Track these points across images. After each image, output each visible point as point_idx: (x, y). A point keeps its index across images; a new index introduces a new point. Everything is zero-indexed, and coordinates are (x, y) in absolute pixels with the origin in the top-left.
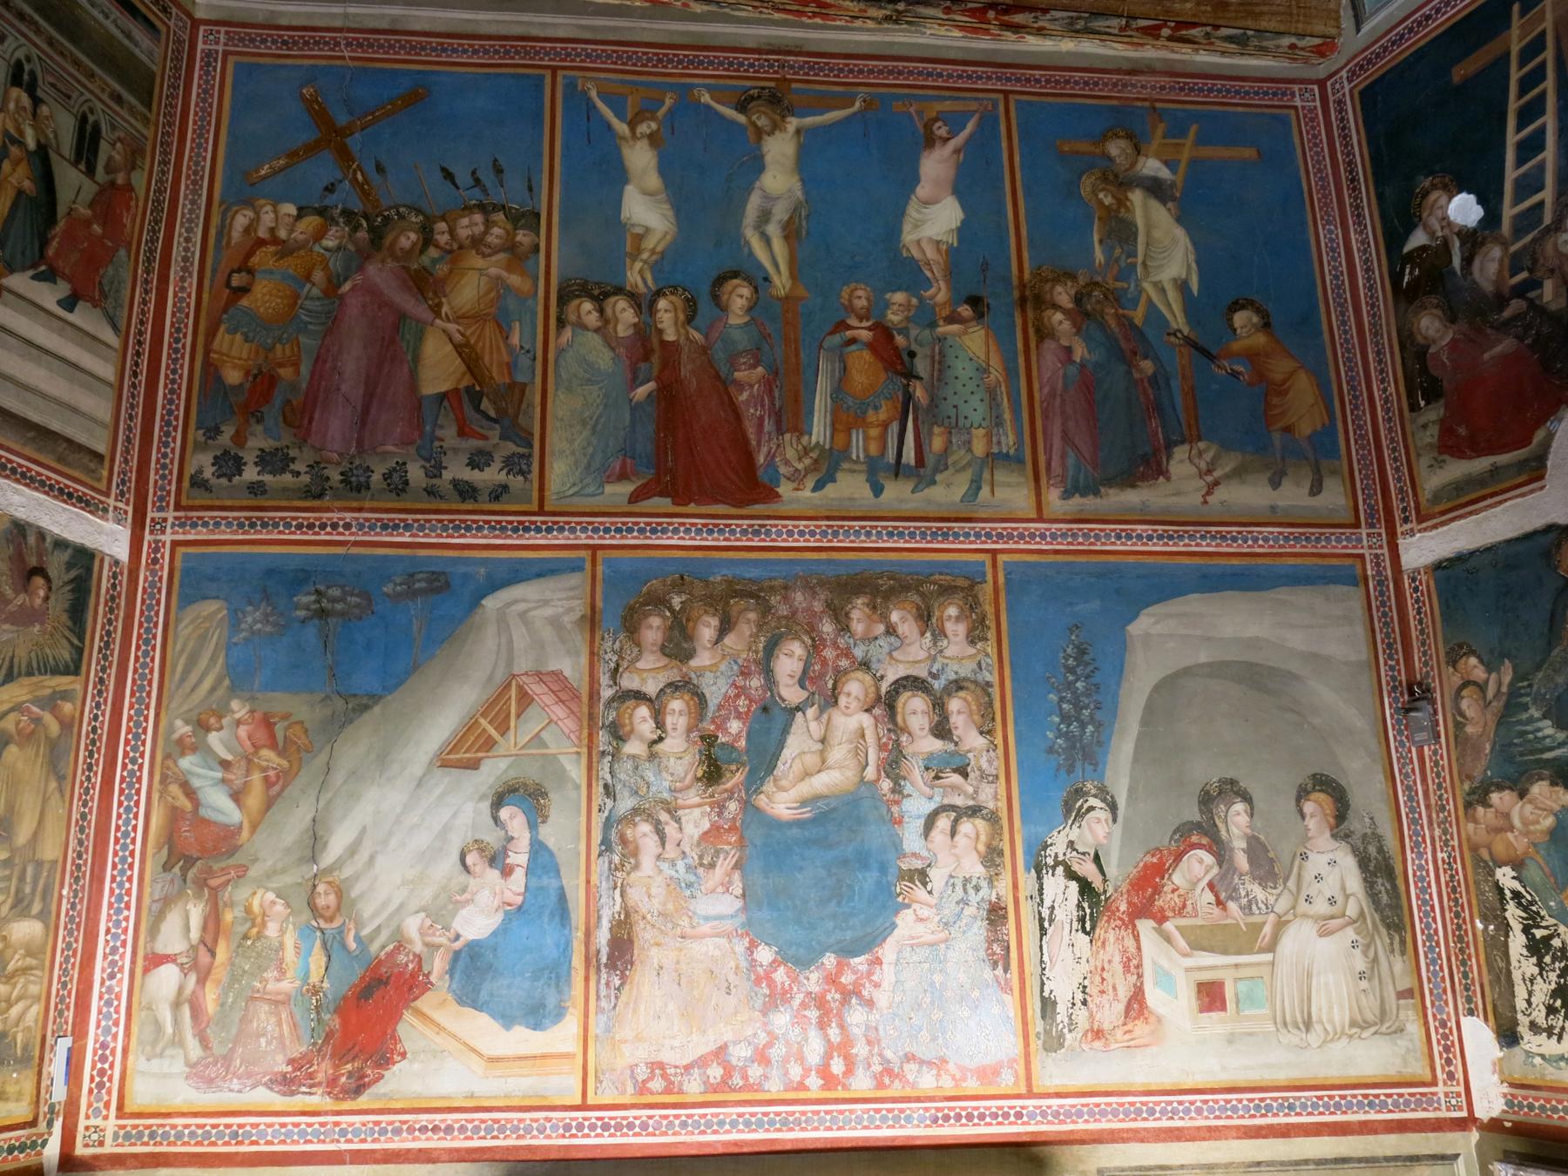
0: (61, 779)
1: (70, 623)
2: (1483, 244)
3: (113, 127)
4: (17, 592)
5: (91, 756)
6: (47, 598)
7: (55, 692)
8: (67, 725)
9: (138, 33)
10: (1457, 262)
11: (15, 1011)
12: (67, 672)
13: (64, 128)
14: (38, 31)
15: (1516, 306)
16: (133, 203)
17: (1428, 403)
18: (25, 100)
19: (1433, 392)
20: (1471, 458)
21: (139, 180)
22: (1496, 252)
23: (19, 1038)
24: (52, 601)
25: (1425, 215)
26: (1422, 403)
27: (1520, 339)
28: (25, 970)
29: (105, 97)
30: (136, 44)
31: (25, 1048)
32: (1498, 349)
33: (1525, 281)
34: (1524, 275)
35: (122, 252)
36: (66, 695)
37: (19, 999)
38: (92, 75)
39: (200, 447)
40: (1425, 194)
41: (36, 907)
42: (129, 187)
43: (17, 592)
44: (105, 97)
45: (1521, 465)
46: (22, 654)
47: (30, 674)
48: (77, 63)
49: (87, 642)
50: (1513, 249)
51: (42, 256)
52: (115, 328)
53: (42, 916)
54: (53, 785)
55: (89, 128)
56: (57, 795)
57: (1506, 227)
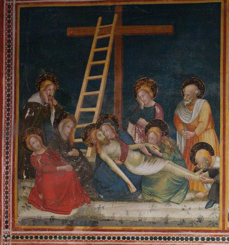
2: (65, 117)
10: (52, 119)
15: (73, 152)
17: (27, 178)
19: (31, 174)
20: (43, 210)
22: (70, 124)
25: (42, 89)
26: (25, 177)
27: (74, 167)
32: (63, 167)
33: (80, 143)
34: (80, 140)
40: (44, 79)
45: (64, 222)
50: (78, 126)
57: (77, 115)
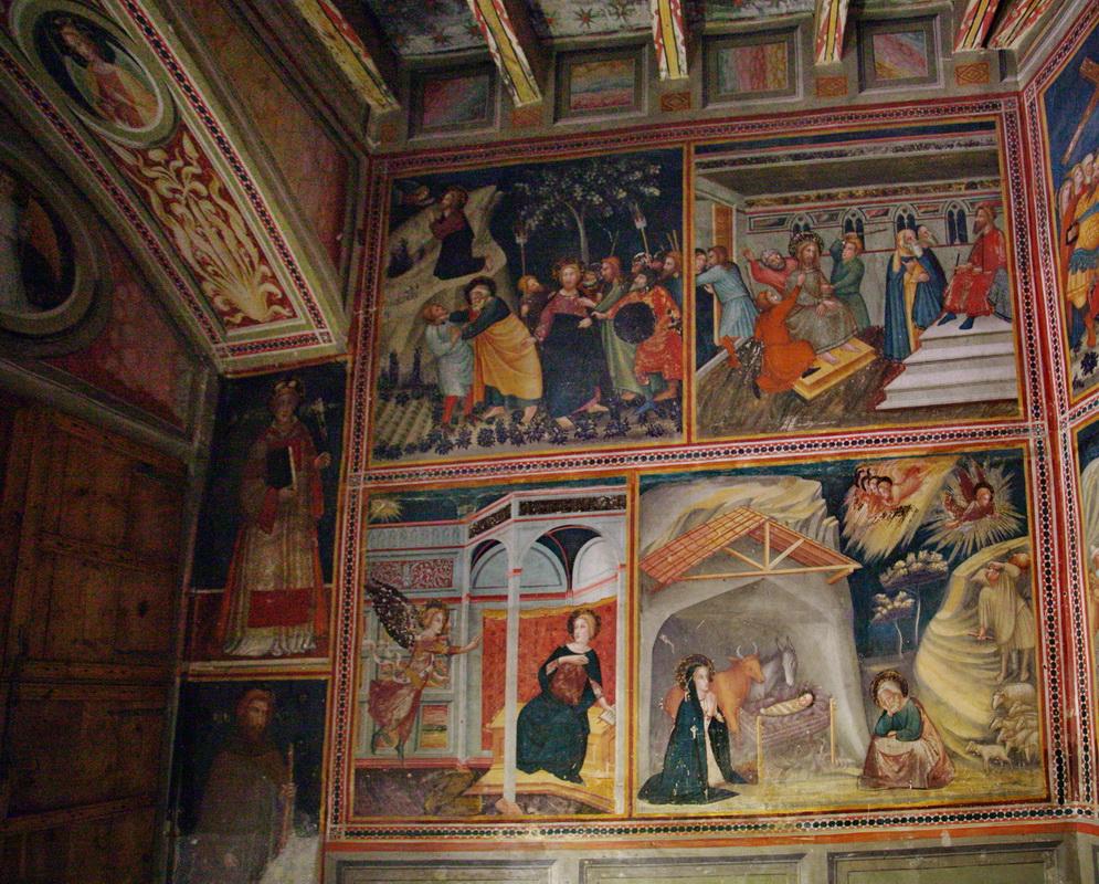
0: (1027, 599)
1: (1012, 507)
3: (972, 204)
4: (969, 502)
5: (1048, 580)
6: (991, 499)
7: (1010, 551)
8: (1025, 568)
9: (976, 137)
11: (1020, 736)
12: (1017, 535)
13: (940, 229)
14: (907, 190)
16: (1001, 238)
18: (909, 233)
21: (1002, 222)
23: (1027, 750)
24: (996, 497)
28: (1023, 712)
29: (963, 192)
30: (977, 144)
31: (1033, 756)
35: (1001, 272)
36: (1018, 550)
37: (1022, 729)
38: (950, 186)
39: (1074, 360)
41: (1024, 676)
42: (995, 229)
43: (969, 502)
44: (963, 192)
46: (981, 536)
47: (989, 543)
48: (936, 188)
49: (1029, 514)
51: (942, 307)
52: (1007, 319)
53: (1030, 680)
54: (1022, 603)
55: (955, 217)
56: (1027, 610)
